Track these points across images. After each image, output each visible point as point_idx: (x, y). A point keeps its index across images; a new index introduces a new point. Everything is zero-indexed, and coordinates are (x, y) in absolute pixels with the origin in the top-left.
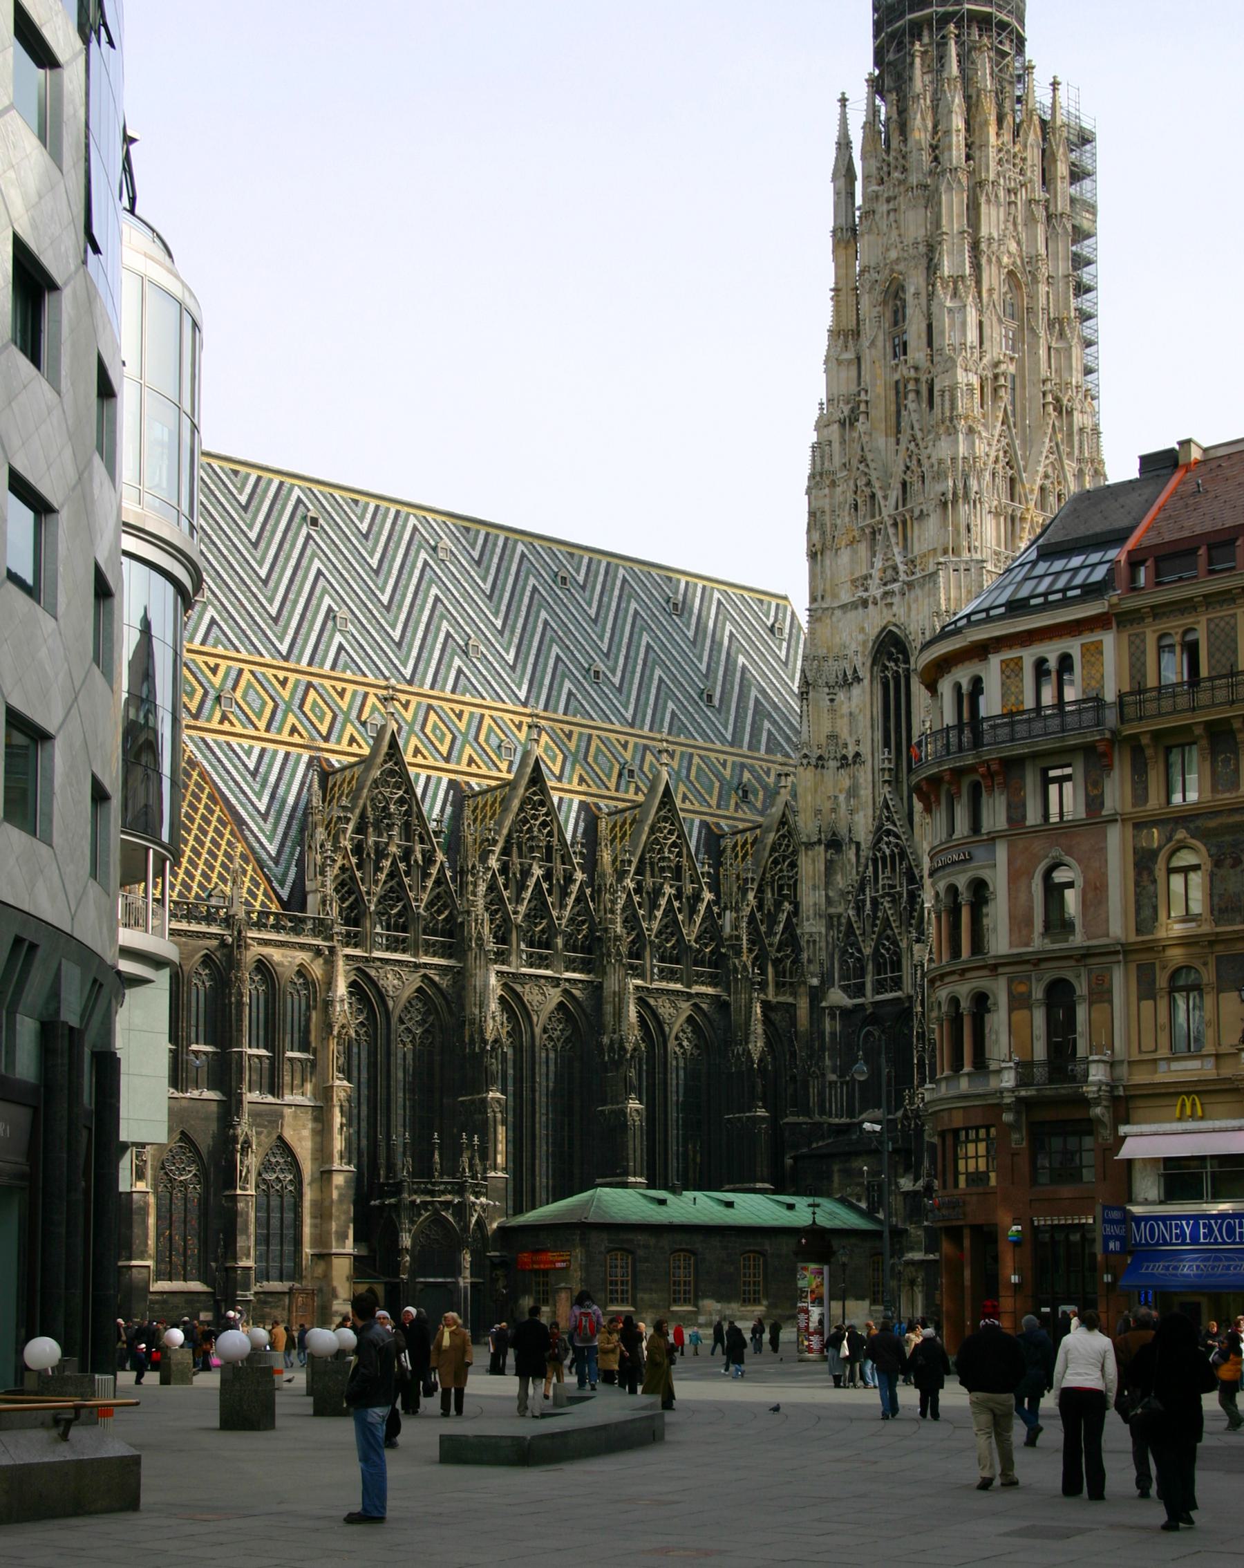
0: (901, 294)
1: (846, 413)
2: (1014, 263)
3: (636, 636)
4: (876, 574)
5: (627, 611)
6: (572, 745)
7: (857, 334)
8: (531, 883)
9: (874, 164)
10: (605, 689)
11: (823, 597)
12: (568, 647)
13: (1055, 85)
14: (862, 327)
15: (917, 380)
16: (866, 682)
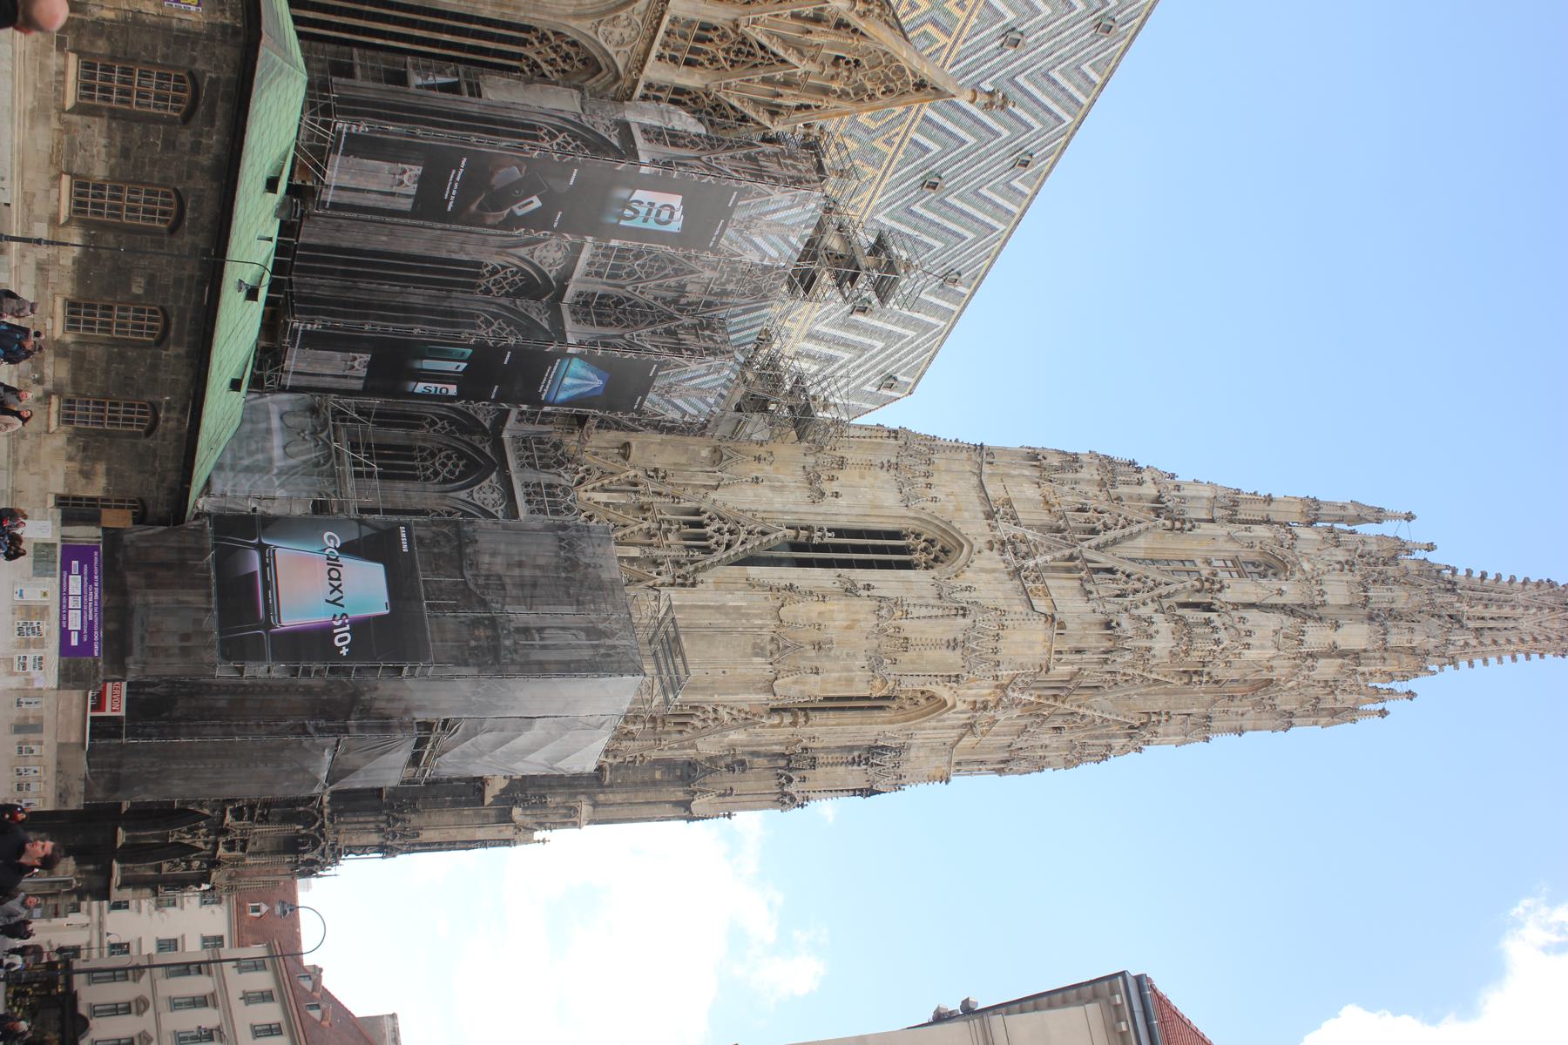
0: (1271, 571)
1: (1168, 504)
2: (1277, 685)
3: (944, 234)
4: (1019, 531)
5: (968, 229)
6: (879, 144)
7: (1231, 521)
8: (793, 59)
9: (1374, 548)
10: (915, 193)
11: (991, 463)
12: (966, 157)
13: (1383, 713)
14: (1243, 526)
15: (1211, 591)
16: (904, 511)
